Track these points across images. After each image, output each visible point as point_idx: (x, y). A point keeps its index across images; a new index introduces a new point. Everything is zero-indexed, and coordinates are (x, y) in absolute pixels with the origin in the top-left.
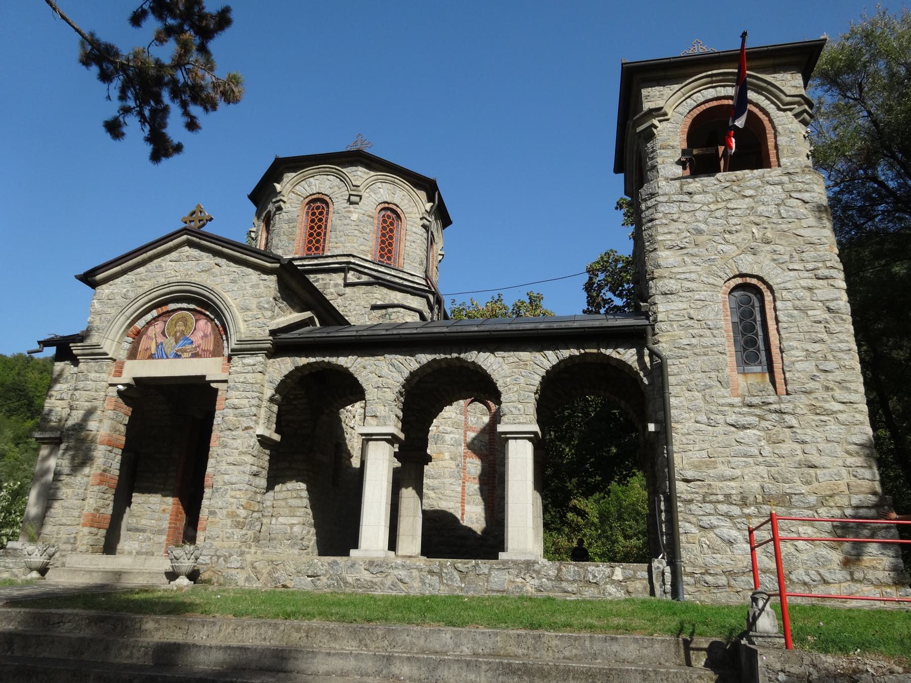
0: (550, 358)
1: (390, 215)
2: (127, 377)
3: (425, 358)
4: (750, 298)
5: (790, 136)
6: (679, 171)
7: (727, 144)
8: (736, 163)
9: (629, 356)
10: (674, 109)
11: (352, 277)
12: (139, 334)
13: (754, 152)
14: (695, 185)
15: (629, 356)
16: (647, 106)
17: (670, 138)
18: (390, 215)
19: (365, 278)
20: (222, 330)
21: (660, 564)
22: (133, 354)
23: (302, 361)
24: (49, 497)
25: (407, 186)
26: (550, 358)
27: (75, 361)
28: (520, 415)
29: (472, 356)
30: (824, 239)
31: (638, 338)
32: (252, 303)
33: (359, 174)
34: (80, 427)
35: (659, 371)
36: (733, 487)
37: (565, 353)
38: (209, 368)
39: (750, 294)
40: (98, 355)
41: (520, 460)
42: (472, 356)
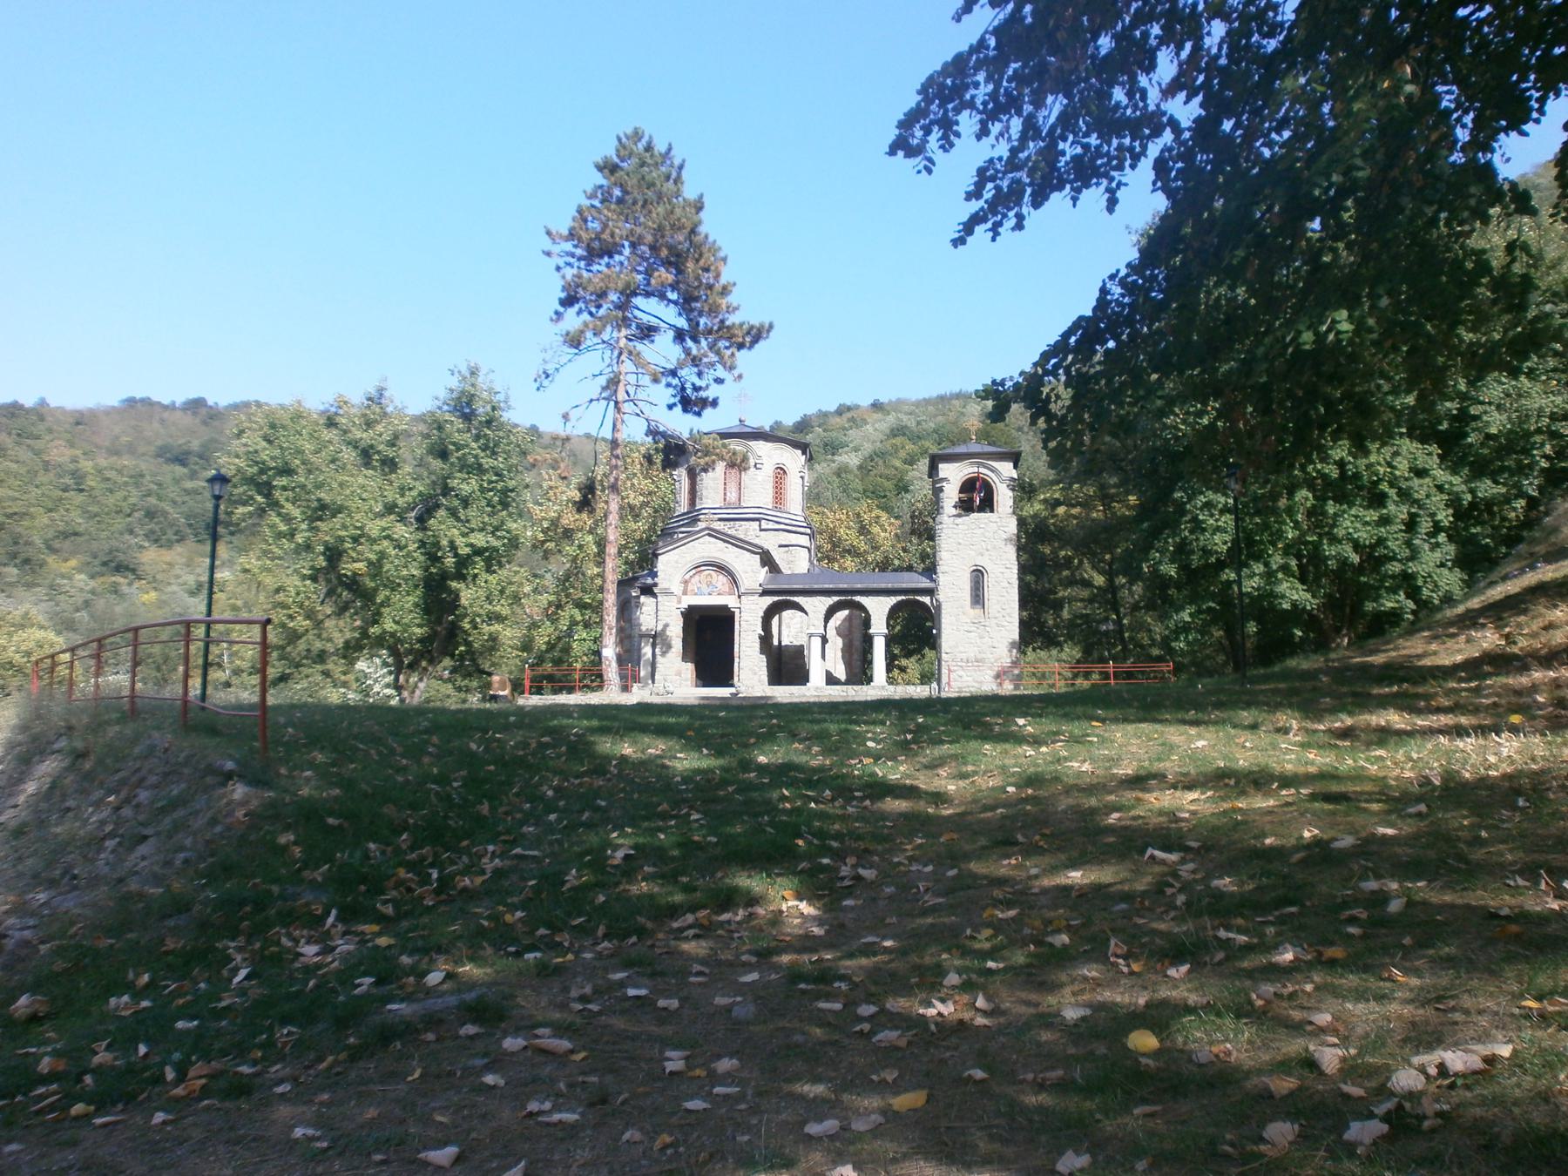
0: (893, 600)
1: (781, 471)
2: (684, 605)
3: (836, 599)
4: (978, 576)
5: (1004, 497)
6: (954, 511)
7: (977, 497)
8: (981, 509)
9: (926, 600)
10: (954, 475)
11: (764, 525)
12: (686, 582)
13: (988, 504)
14: (959, 520)
15: (926, 600)
16: (941, 475)
17: (951, 494)
18: (781, 471)
19: (771, 525)
20: (734, 581)
21: (934, 685)
22: (685, 593)
23: (776, 598)
24: (653, 665)
25: (789, 449)
26: (893, 600)
27: (654, 595)
28: (879, 627)
29: (858, 598)
30: (1011, 554)
31: (930, 592)
32: (752, 573)
33: (760, 447)
34: (664, 630)
35: (938, 608)
36: (964, 656)
37: (900, 598)
38: (730, 601)
39: (978, 576)
40: (668, 593)
41: (879, 646)
42: (858, 598)
